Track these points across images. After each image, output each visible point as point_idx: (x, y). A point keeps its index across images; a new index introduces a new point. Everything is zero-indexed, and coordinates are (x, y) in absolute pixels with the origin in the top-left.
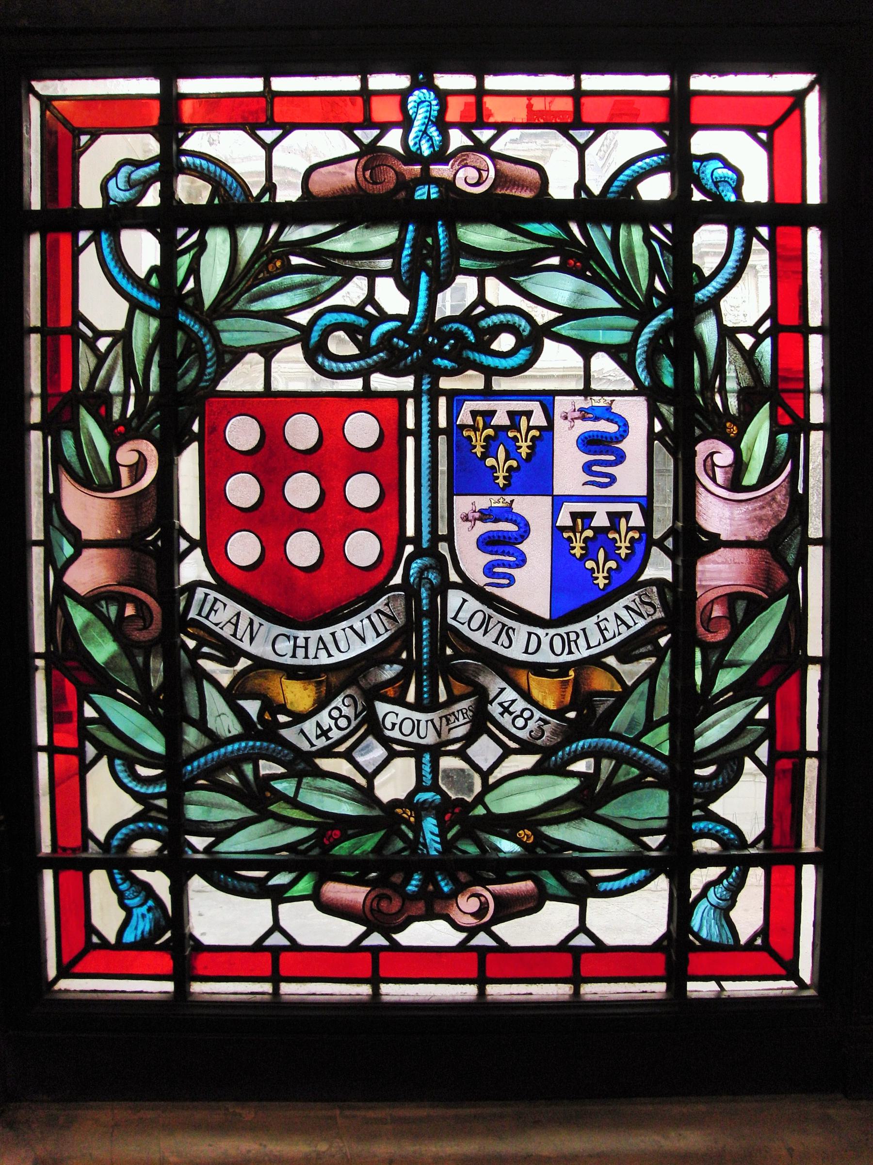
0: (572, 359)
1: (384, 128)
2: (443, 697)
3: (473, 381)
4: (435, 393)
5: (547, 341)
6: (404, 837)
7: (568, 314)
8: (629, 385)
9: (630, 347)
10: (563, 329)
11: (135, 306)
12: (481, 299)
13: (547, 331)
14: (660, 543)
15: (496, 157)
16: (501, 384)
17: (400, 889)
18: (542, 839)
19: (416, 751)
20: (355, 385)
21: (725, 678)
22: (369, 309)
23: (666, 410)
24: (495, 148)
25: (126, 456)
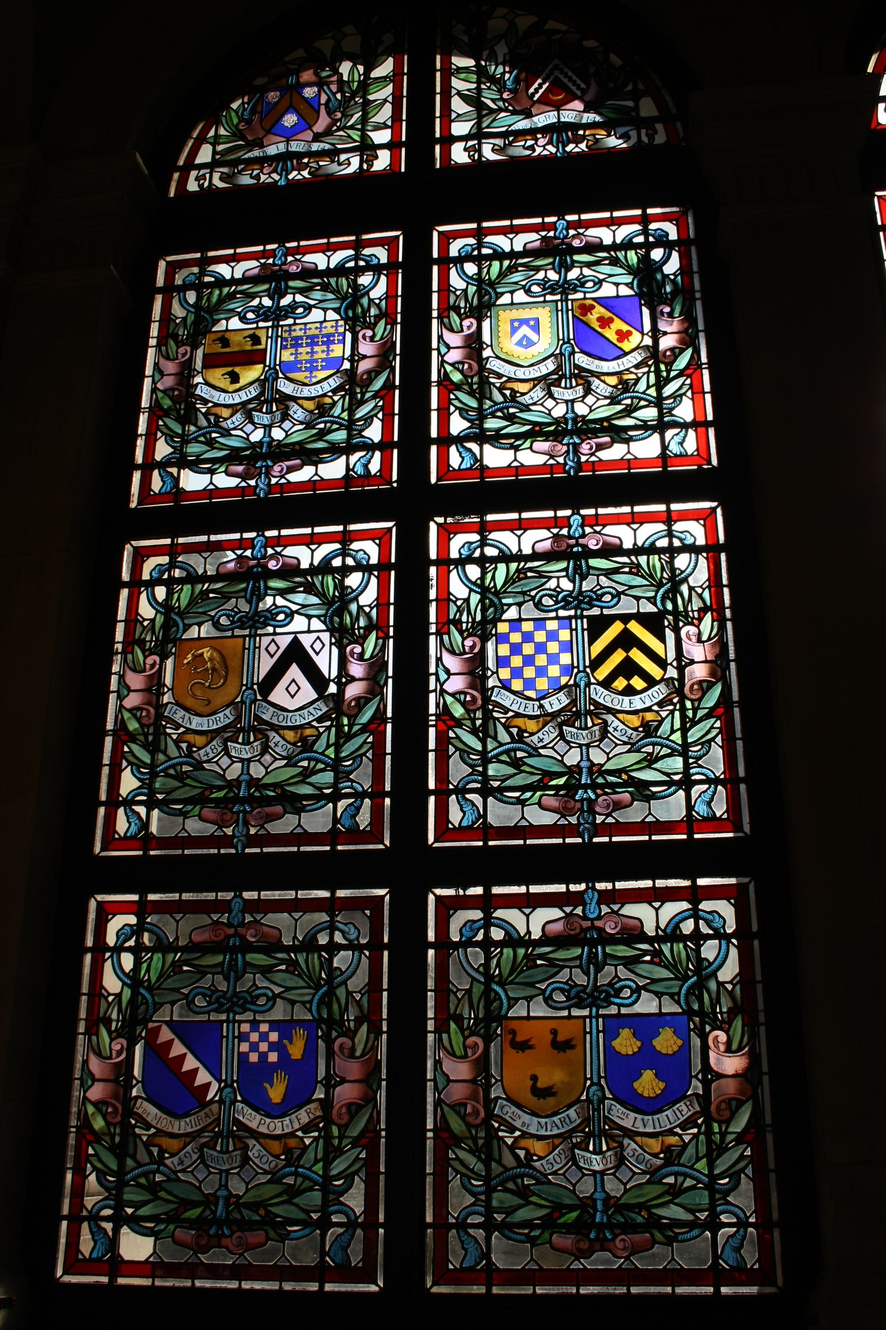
0: (306, 620)
1: (245, 550)
2: (252, 739)
3: (270, 629)
4: (256, 635)
5: (296, 615)
6: (234, 792)
7: (304, 606)
8: (324, 628)
9: (325, 616)
10: (301, 611)
11: (157, 611)
12: (274, 604)
13: (297, 612)
14: (333, 681)
15: (283, 556)
16: (278, 630)
17: (231, 810)
18: (284, 791)
19: (242, 760)
20: (229, 634)
21: (356, 728)
22: (235, 610)
23: (337, 635)
24: (283, 553)
25: (150, 661)
